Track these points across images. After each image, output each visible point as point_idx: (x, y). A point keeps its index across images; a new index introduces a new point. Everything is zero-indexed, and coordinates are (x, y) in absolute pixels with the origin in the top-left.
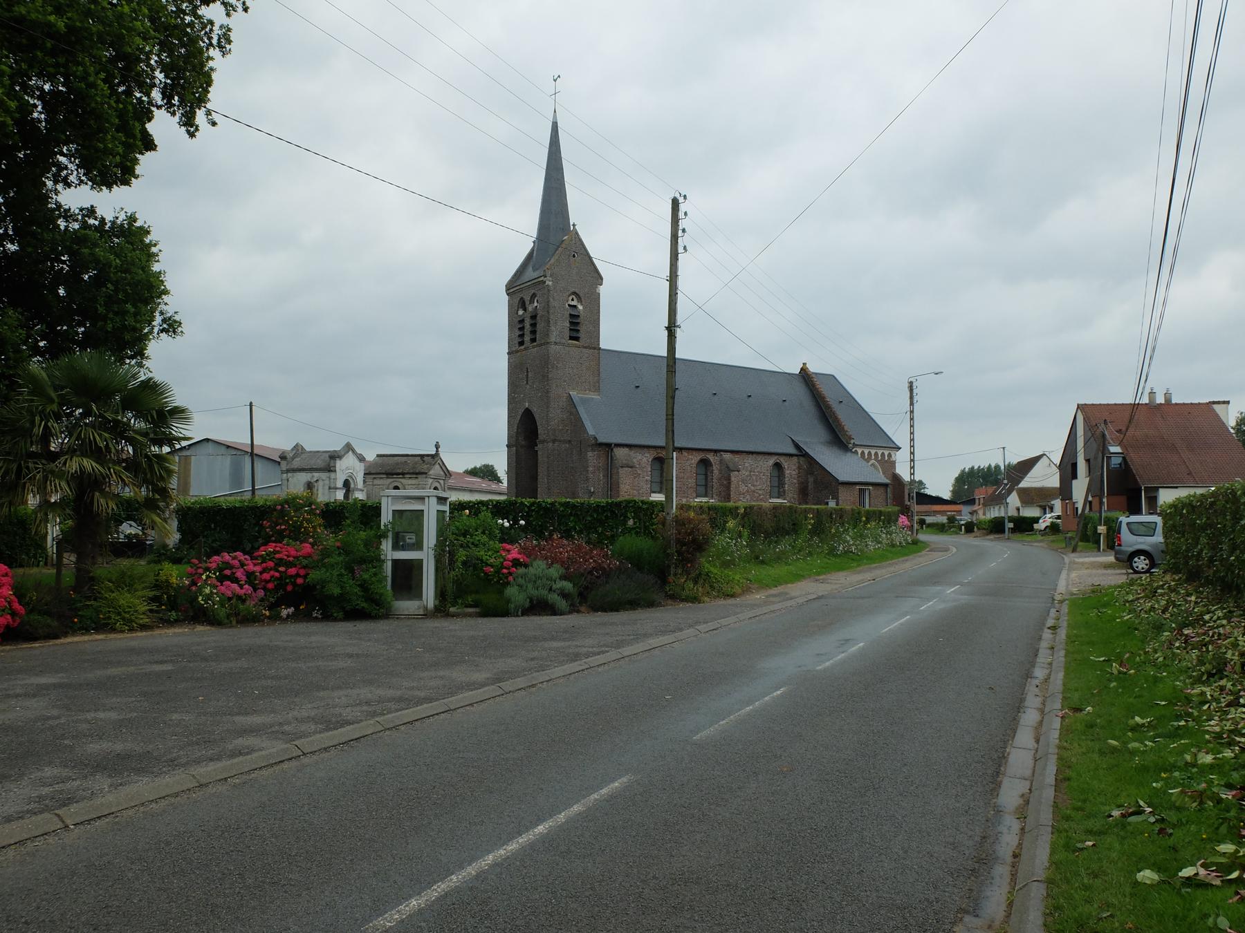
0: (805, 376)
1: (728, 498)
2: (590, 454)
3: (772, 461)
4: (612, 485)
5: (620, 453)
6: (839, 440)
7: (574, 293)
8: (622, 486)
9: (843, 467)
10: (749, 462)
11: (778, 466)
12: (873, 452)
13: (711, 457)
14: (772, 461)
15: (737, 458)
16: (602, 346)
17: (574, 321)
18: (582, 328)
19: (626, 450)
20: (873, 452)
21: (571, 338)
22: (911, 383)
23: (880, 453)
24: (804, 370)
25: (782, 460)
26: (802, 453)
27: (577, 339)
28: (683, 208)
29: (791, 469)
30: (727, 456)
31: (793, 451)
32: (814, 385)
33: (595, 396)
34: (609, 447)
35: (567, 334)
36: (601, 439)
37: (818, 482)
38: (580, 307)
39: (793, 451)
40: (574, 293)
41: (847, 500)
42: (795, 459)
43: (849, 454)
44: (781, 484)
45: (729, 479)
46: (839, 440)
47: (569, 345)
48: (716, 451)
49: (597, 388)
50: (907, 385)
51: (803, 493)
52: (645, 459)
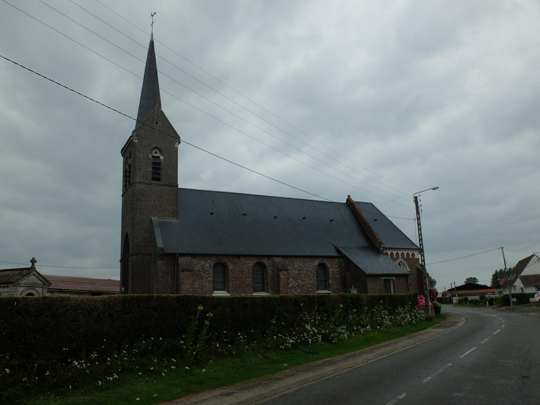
0: (350, 203)
1: (278, 292)
2: (159, 262)
3: (317, 262)
4: (177, 287)
5: (183, 261)
6: (373, 246)
7: (156, 148)
8: (183, 286)
9: (370, 264)
10: (298, 263)
11: (322, 266)
12: (400, 253)
13: (265, 261)
14: (317, 262)
15: (287, 261)
16: (182, 184)
17: (156, 166)
18: (163, 172)
19: (189, 258)
20: (400, 253)
21: (153, 179)
22: (416, 198)
23: (405, 253)
24: (349, 200)
25: (325, 261)
26: (341, 256)
27: (159, 179)
29: (333, 268)
30: (277, 260)
31: (335, 254)
32: (355, 209)
33: (174, 220)
34: (173, 257)
35: (150, 176)
36: (167, 251)
37: (352, 274)
38: (162, 157)
39: (335, 254)
40: (156, 148)
41: (374, 289)
42: (336, 260)
43: (381, 255)
44: (326, 279)
45: (278, 277)
46: (373, 246)
47: (151, 184)
48: (269, 257)
49: (176, 215)
50: (413, 199)
51: (344, 285)
52: (208, 264)
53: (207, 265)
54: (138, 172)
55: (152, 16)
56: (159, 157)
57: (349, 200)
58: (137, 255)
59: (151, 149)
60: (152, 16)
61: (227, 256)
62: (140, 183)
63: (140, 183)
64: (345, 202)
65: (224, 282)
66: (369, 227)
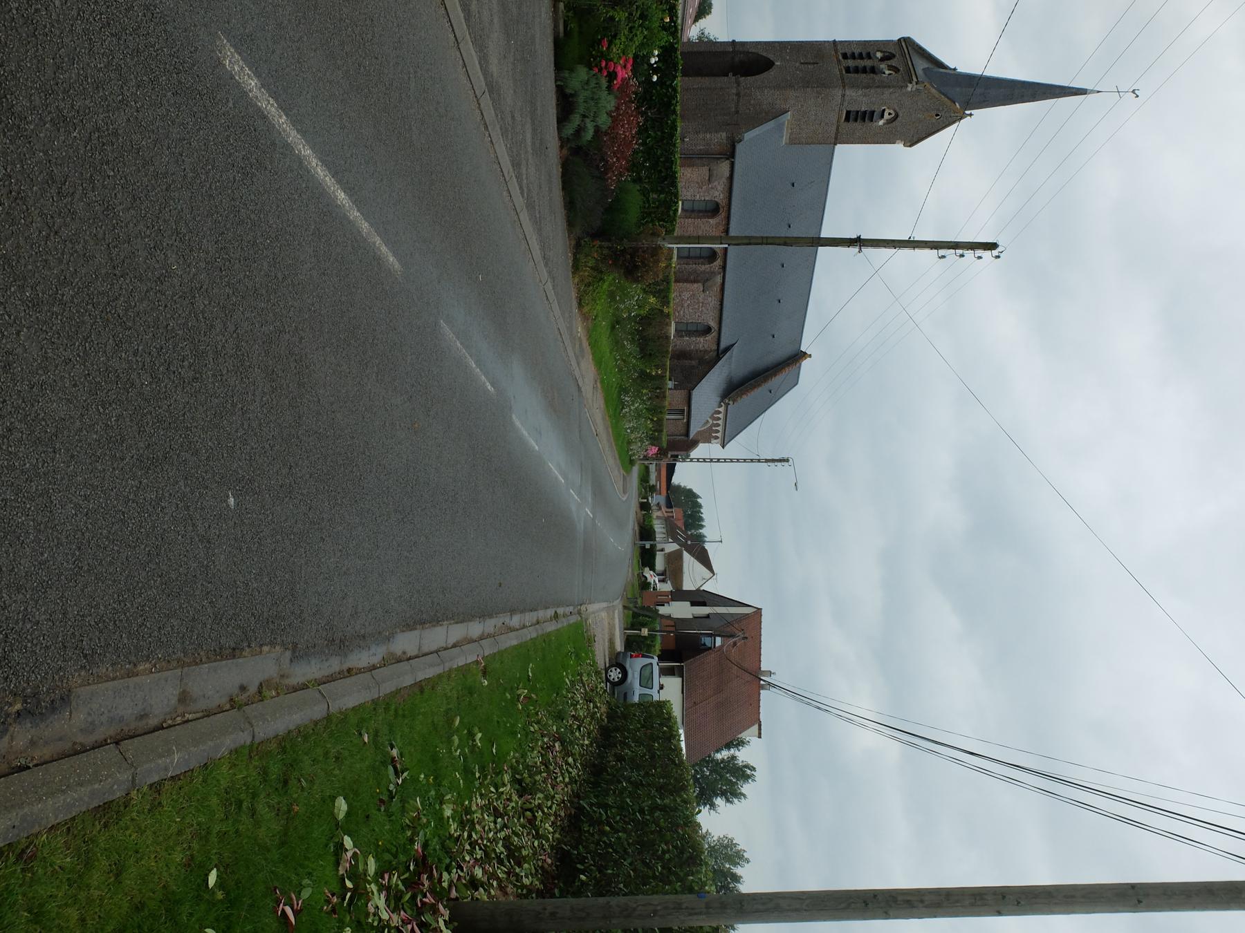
0: (798, 357)
1: (677, 281)
2: (724, 135)
3: (713, 324)
4: (692, 159)
5: (724, 167)
6: (733, 390)
7: (897, 116)
8: (689, 170)
9: (706, 395)
10: (713, 302)
11: (708, 330)
12: (720, 422)
13: (718, 262)
14: (713, 324)
15: (717, 288)
16: (839, 147)
17: (867, 116)
18: (858, 125)
19: (727, 174)
20: (720, 422)
21: (848, 113)
22: (787, 460)
23: (719, 428)
24: (804, 355)
25: (714, 334)
26: (720, 354)
27: (847, 119)
28: (987, 255)
29: (704, 343)
30: (719, 279)
31: (723, 346)
32: (788, 365)
33: (785, 140)
34: (730, 155)
35: (854, 108)
36: (739, 147)
37: (692, 370)
38: (881, 123)
39: (723, 346)
40: (897, 116)
41: (673, 397)
42: (715, 347)
43: (719, 399)
44: (690, 333)
45: (695, 281)
46: (733, 390)
47: (841, 110)
48: (724, 268)
49: (793, 141)
50: (786, 457)
51: (681, 355)
52: (718, 194)
53: (717, 194)
54: (860, 92)
55: (1133, 92)
56: (882, 116)
57: (804, 355)
58: (738, 94)
59: (901, 89)
60: (1133, 92)
61: (728, 218)
62: (843, 96)
63: (843, 96)
64: (803, 349)
65: (693, 211)
66: (759, 385)
